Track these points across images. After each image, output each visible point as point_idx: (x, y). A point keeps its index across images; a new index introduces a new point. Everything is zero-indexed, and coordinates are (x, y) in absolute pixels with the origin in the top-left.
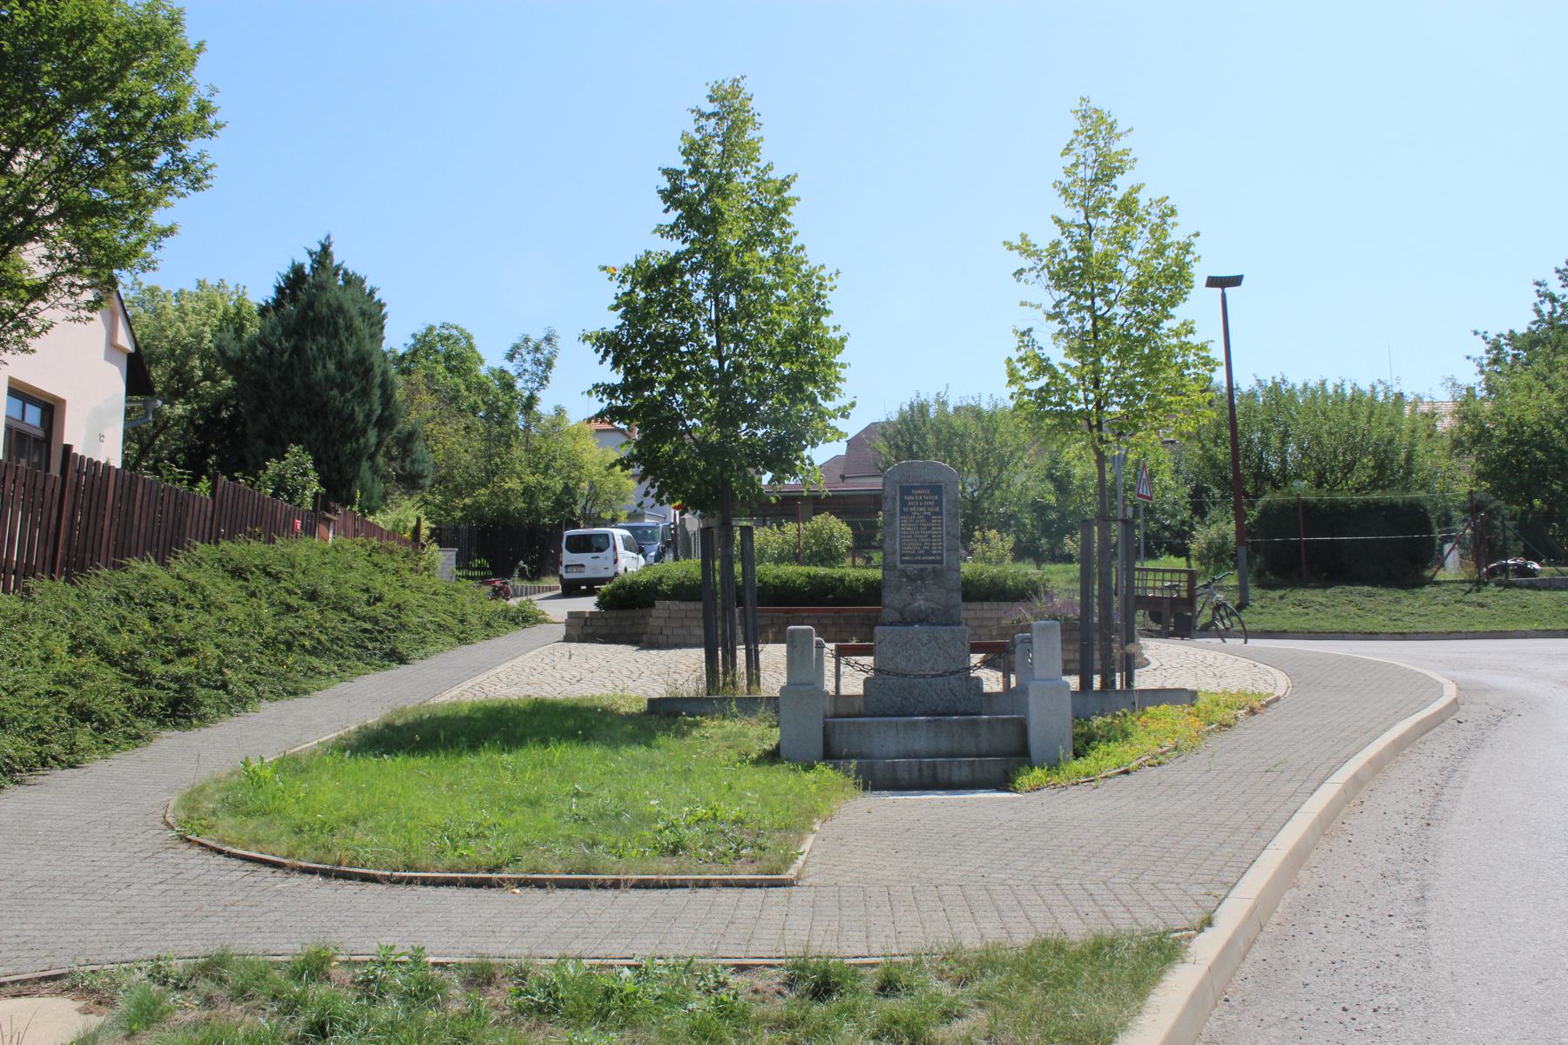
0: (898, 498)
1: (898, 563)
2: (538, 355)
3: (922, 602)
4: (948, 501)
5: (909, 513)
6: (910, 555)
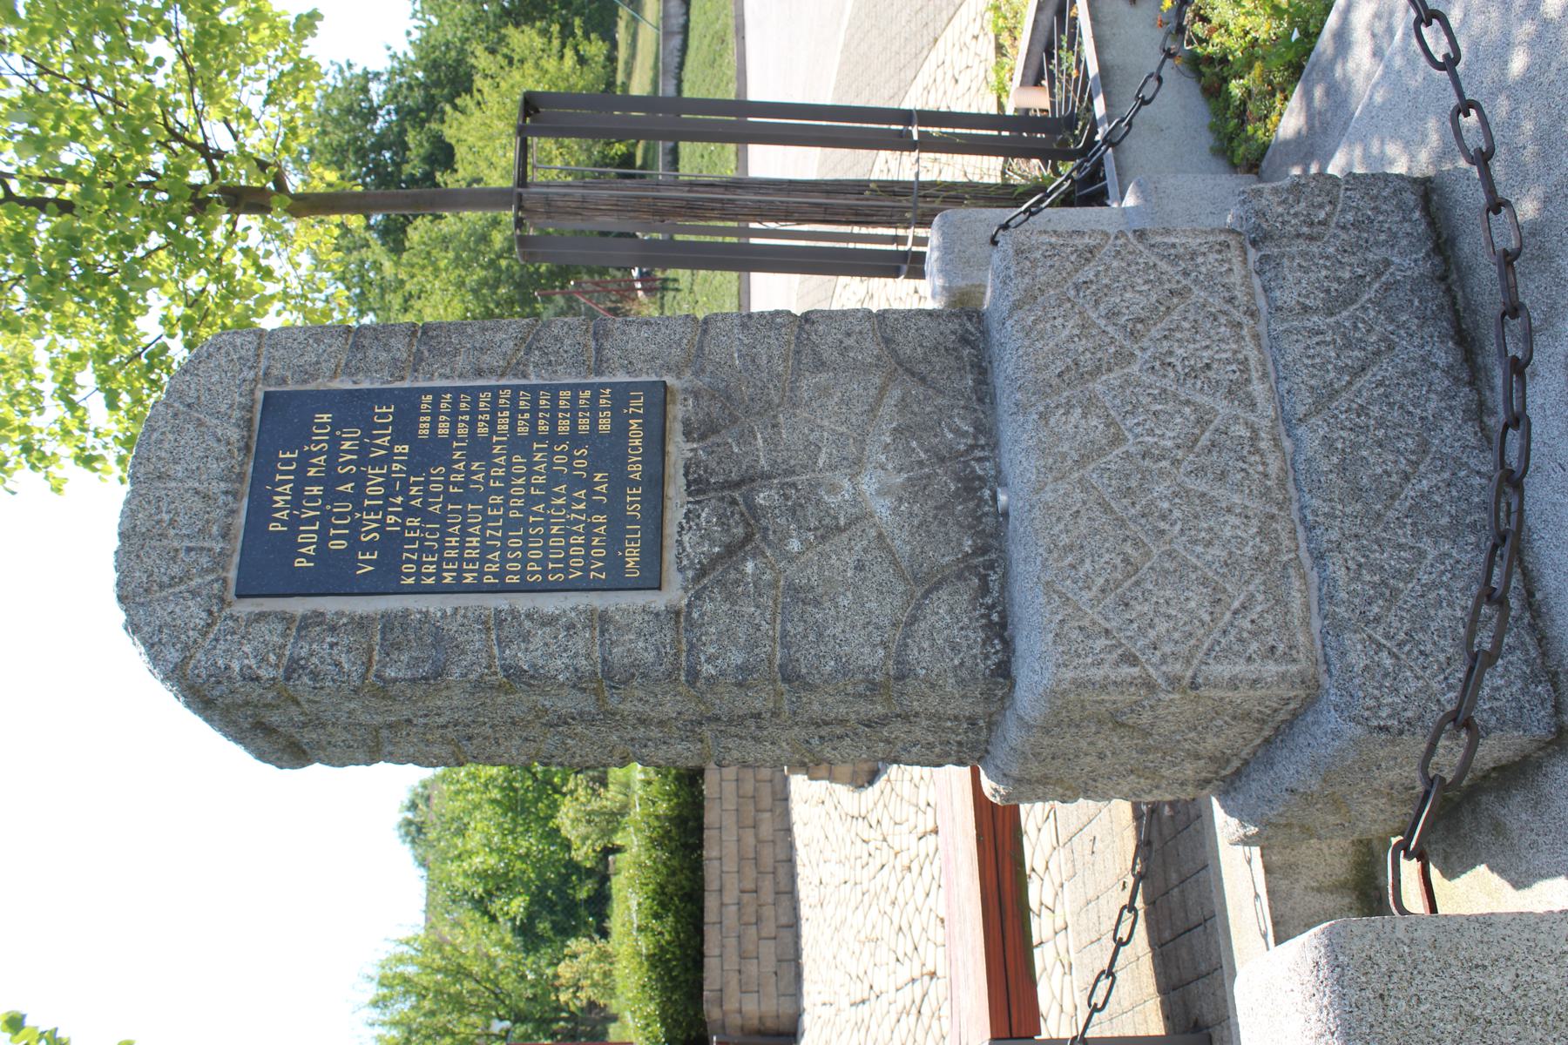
0: (299, 606)
3: (868, 484)
4: (349, 370)
5: (391, 544)
6: (615, 540)
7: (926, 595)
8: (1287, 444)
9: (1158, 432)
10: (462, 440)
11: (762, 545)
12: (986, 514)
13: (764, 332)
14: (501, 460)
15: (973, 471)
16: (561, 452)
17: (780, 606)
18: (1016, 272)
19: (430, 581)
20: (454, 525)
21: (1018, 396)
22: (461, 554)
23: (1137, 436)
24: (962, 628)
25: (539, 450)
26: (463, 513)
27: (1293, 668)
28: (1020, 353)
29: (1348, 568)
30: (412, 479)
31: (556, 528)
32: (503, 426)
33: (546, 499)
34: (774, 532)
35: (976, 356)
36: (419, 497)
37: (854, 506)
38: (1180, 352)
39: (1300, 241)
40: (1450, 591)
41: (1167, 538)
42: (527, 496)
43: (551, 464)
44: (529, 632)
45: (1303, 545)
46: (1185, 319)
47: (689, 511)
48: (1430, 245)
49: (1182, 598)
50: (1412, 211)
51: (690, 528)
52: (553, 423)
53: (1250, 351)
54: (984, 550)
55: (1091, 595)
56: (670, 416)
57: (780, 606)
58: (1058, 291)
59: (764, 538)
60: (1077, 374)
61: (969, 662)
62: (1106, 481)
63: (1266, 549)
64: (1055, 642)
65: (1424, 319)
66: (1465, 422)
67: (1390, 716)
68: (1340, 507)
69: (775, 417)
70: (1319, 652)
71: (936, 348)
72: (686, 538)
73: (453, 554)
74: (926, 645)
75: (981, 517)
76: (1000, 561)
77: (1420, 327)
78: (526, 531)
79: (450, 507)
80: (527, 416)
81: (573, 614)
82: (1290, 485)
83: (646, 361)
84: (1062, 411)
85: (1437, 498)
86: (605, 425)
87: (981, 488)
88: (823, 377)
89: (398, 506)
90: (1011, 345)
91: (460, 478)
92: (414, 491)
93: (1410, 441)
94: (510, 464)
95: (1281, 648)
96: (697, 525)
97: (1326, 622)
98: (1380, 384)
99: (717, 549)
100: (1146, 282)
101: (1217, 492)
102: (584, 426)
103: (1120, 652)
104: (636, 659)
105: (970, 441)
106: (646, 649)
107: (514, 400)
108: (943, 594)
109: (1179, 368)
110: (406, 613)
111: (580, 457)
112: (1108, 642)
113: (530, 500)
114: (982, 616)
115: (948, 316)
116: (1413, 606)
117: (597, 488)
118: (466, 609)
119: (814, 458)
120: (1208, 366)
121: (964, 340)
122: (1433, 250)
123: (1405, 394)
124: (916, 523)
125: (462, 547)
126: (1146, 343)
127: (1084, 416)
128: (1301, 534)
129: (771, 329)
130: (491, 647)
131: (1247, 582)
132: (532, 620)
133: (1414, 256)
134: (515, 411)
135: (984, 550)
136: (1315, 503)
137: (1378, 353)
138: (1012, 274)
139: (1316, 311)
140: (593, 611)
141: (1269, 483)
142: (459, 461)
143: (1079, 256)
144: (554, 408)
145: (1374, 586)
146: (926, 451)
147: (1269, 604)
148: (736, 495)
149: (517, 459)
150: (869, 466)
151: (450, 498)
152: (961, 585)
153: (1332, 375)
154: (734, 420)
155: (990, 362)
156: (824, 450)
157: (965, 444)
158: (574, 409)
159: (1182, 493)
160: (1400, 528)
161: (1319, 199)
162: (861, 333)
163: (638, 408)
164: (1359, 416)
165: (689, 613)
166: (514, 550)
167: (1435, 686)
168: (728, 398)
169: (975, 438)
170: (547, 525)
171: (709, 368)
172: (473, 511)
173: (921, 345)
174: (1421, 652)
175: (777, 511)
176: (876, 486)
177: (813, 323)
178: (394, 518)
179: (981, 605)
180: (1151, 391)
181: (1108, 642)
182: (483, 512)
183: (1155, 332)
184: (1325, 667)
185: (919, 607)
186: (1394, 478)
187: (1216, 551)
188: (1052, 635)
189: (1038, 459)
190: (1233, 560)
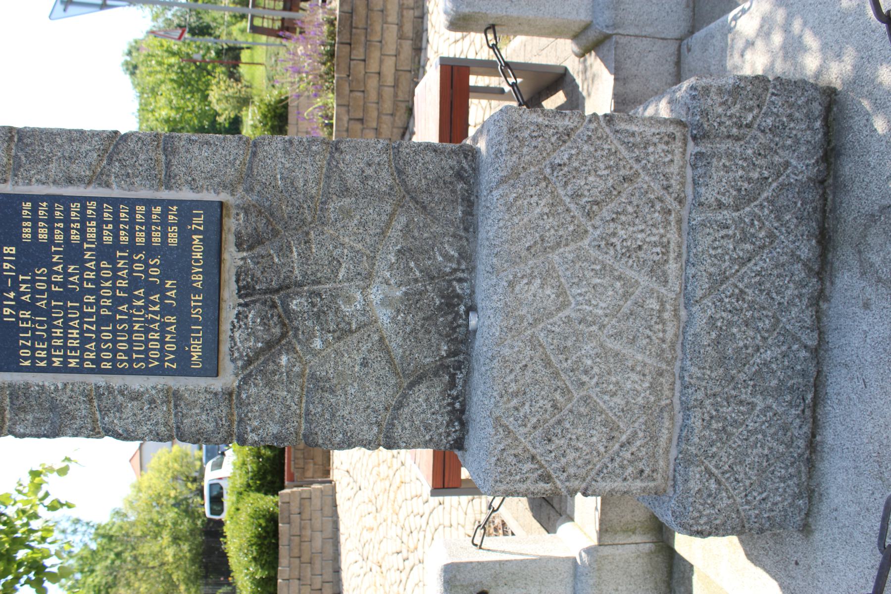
1: (217, 384)
2: (69, 531)
3: (375, 294)
6: (183, 338)
7: (411, 385)
8: (683, 313)
9: (593, 302)
10: (59, 245)
11: (294, 341)
12: (459, 326)
13: (302, 158)
14: (91, 265)
15: (454, 290)
16: (139, 261)
17: (305, 390)
18: (507, 150)
19: (43, 364)
20: (57, 318)
21: (495, 260)
22: (65, 343)
23: (578, 303)
24: (433, 414)
25: (121, 258)
26: (65, 308)
27: (652, 484)
28: (501, 224)
29: (703, 420)
30: (21, 277)
31: (138, 325)
32: (92, 235)
33: (129, 301)
34: (303, 332)
35: (467, 191)
36: (28, 293)
37: (364, 315)
38: (622, 233)
39: (730, 140)
40: (765, 436)
41: (585, 387)
42: (114, 297)
43: (131, 271)
44: (121, 404)
45: (677, 394)
46: (630, 203)
47: (239, 313)
48: (821, 153)
49: (588, 435)
50: (816, 119)
51: (240, 326)
52: (132, 234)
53: (673, 236)
54: (454, 354)
55: (526, 430)
56: (225, 228)
57: (305, 390)
58: (537, 169)
59: (296, 336)
60: (543, 247)
61: (436, 438)
62: (549, 340)
63: (652, 399)
64: (496, 464)
65: (800, 219)
66: (807, 307)
67: (706, 523)
68: (708, 372)
69: (307, 234)
70: (671, 473)
71: (437, 181)
72: (237, 335)
73: (59, 343)
74: (407, 425)
75: (456, 328)
76: (466, 362)
77: (796, 226)
78: (115, 326)
79: (53, 303)
80: (110, 227)
81: (154, 392)
82: (678, 347)
83: (206, 178)
84: (525, 281)
85: (774, 366)
86: (173, 239)
87: (459, 305)
88: (347, 201)
89: (11, 300)
90: (494, 214)
91: (59, 278)
92: (23, 288)
93: (767, 322)
94: (98, 269)
95: (647, 471)
96: (245, 324)
97: (680, 456)
98: (758, 274)
99: (260, 345)
100: (606, 168)
101: (627, 351)
102: (156, 238)
103: (539, 472)
104: (200, 429)
105: (454, 266)
106: (208, 421)
107: (99, 211)
108: (423, 387)
109: (618, 247)
110: (27, 386)
111: (154, 266)
112: (532, 466)
113: (117, 301)
114: (449, 404)
115: (449, 153)
116: (739, 446)
117: (168, 294)
118: (73, 384)
119: (336, 272)
120: (640, 248)
121: (459, 175)
122: (822, 157)
123: (773, 283)
124: (408, 330)
125: (65, 338)
126: (597, 222)
127: (542, 286)
128: (678, 386)
129: (307, 155)
130: (94, 414)
131: (634, 422)
132: (123, 395)
133: (807, 162)
134: (101, 222)
135: (454, 354)
136: (693, 369)
137: (762, 247)
138: (503, 150)
139: (727, 207)
140: (170, 388)
141: (664, 346)
142: (57, 264)
143: (559, 139)
144: (132, 222)
145: (717, 431)
146: (421, 271)
147: (646, 440)
148: (276, 298)
149: (104, 264)
150: (377, 280)
151: (53, 296)
152: (436, 380)
153: (727, 263)
154: (275, 233)
155: (477, 197)
156: (344, 265)
157: (451, 267)
158: (148, 223)
159: (604, 353)
160: (744, 388)
161: (751, 102)
162: (379, 164)
163: (199, 225)
164: (737, 301)
165: (239, 394)
166: (106, 342)
167: (738, 500)
168: (272, 214)
169: (459, 263)
170: (130, 322)
171: (258, 188)
172: (72, 308)
173: (425, 178)
174: (736, 479)
175: (306, 315)
176: (381, 296)
177: (342, 152)
178: (9, 310)
179: (449, 395)
180: (594, 267)
181: (532, 466)
182: (80, 309)
183: (606, 214)
184: (672, 483)
185: (404, 396)
186: (750, 351)
187: (618, 400)
188: (495, 458)
189: (502, 321)
190: (628, 407)
